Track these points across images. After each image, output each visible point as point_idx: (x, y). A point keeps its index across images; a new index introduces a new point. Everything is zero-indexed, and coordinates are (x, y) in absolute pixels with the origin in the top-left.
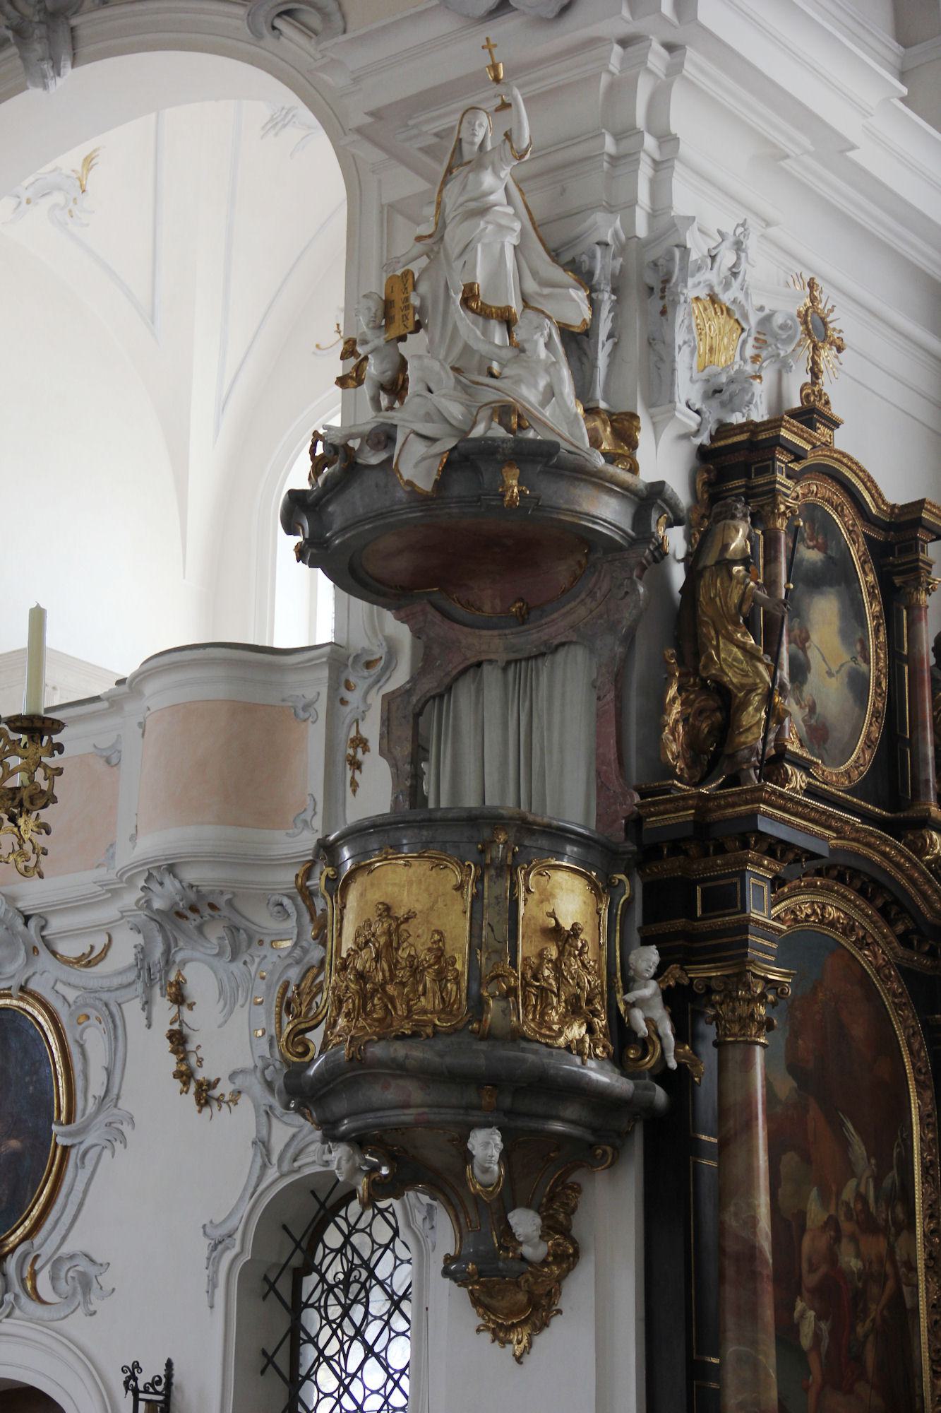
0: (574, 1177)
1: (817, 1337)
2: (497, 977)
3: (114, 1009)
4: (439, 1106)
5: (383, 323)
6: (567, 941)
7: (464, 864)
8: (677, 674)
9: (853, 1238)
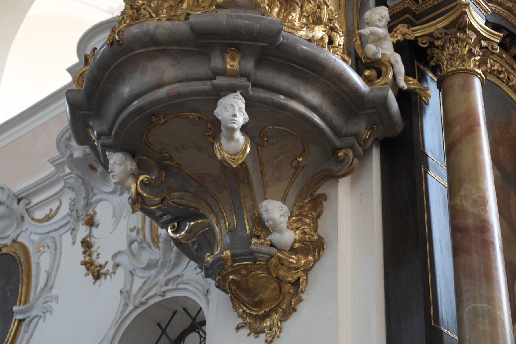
3: (57, 239)
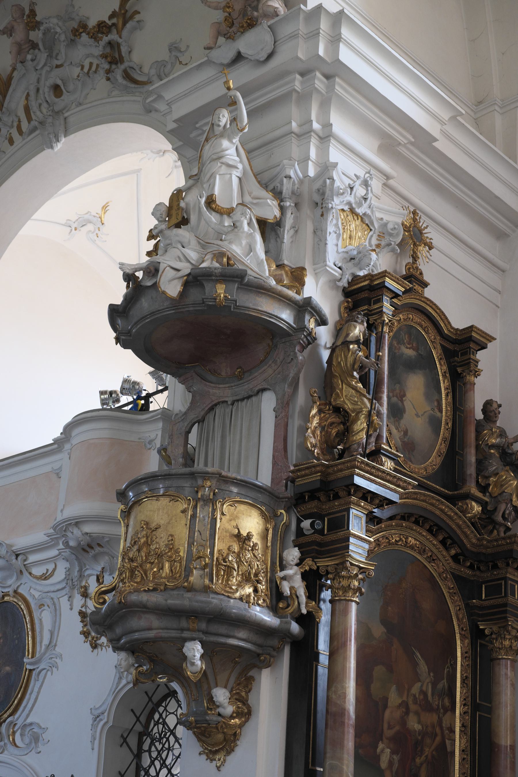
0: (251, 674)
1: (391, 763)
2: (200, 557)
3: (56, 601)
4: (167, 629)
5: (167, 219)
6: (244, 542)
7: (187, 498)
8: (318, 403)
9: (417, 713)
